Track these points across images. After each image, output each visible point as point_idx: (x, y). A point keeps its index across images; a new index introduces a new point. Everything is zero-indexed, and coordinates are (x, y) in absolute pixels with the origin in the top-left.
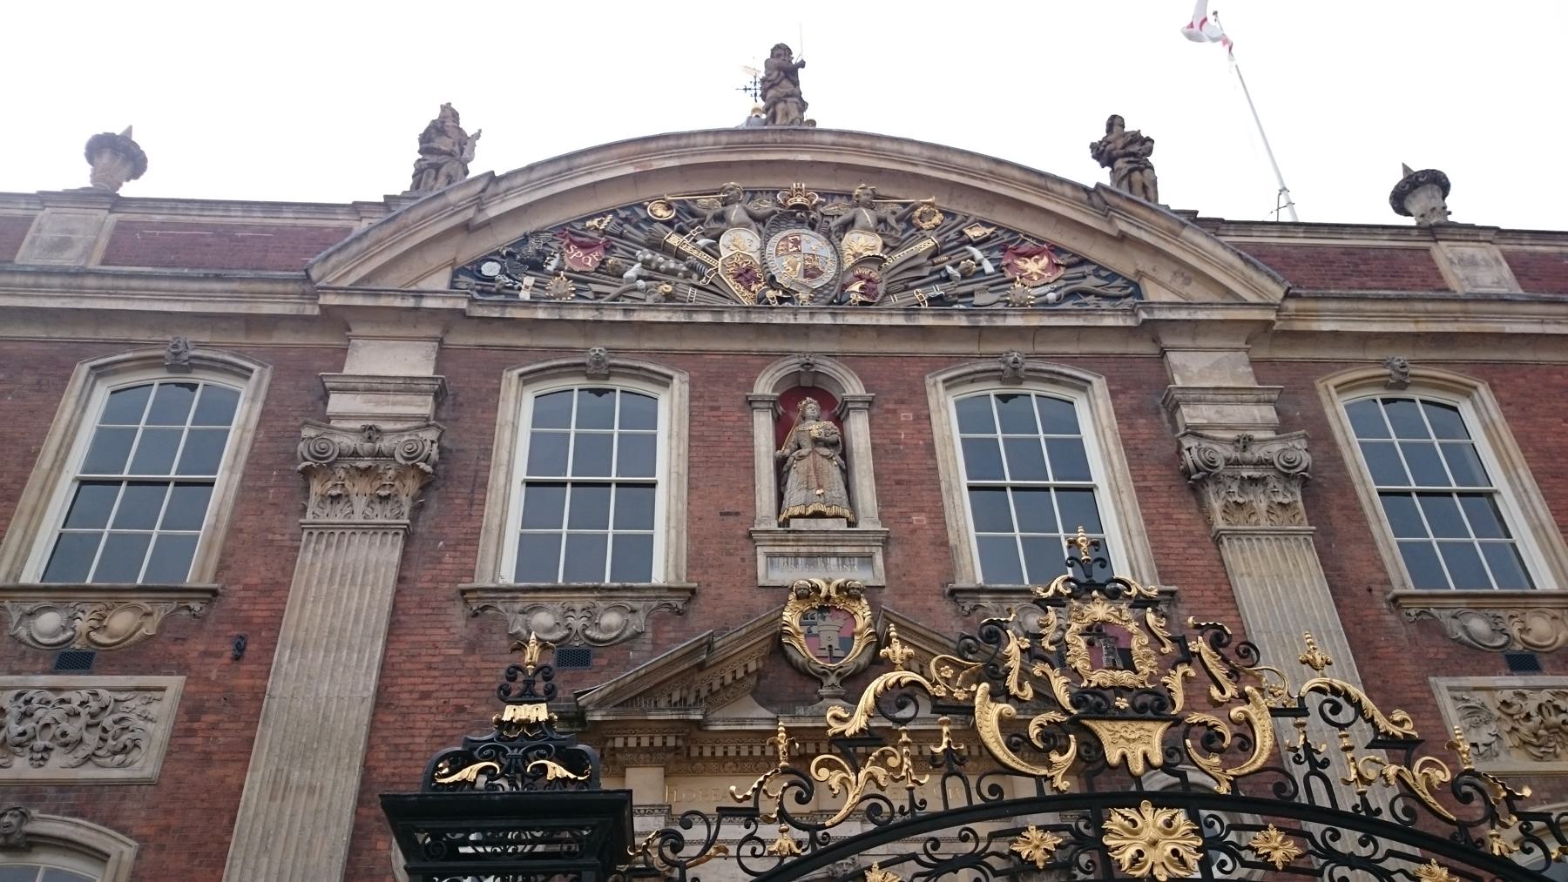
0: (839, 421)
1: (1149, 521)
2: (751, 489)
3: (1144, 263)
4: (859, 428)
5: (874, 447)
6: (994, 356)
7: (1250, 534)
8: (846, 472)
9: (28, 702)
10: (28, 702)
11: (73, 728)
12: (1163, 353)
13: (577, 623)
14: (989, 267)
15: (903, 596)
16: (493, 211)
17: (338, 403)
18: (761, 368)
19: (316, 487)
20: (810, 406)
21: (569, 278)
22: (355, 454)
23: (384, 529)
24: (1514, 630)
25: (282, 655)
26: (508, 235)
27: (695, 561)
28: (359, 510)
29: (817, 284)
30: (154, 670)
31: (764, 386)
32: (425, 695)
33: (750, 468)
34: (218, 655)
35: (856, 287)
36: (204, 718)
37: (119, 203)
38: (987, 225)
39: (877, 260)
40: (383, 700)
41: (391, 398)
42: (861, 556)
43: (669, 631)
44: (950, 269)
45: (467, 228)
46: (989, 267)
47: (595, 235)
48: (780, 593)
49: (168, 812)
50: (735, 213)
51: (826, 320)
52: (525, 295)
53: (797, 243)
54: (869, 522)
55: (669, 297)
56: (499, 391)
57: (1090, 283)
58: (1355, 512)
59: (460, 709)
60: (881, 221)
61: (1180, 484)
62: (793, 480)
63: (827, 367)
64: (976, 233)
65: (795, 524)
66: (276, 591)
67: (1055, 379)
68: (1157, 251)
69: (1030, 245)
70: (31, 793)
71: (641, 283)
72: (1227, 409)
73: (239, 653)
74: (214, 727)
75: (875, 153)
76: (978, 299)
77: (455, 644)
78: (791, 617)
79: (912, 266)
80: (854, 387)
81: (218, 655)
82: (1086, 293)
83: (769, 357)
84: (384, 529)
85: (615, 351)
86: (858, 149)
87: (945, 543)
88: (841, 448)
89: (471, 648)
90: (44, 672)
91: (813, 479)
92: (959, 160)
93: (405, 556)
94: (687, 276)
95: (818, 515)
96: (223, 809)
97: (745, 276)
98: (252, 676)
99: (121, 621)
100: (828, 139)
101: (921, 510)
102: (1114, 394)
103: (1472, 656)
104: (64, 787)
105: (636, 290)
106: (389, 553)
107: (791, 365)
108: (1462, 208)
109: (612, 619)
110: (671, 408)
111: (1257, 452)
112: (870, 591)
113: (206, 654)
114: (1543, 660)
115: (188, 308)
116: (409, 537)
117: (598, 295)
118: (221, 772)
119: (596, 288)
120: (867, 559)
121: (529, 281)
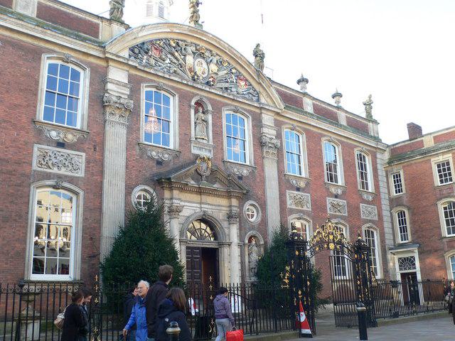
1: (254, 151)
3: (261, 90)
6: (234, 106)
9: (55, 154)
11: (67, 163)
12: (261, 113)
13: (161, 156)
17: (109, 86)
19: (108, 110)
23: (123, 124)
25: (107, 153)
26: (139, 41)
27: (180, 145)
28: (116, 118)
29: (204, 76)
30: (78, 150)
31: (193, 103)
33: (190, 124)
34: (91, 149)
35: (211, 79)
39: (217, 74)
40: (127, 167)
48: (197, 157)
50: (190, 49)
52: (144, 61)
55: (175, 72)
57: (251, 91)
62: (197, 128)
63: (204, 100)
64: (234, 71)
66: (102, 134)
67: (243, 114)
70: (59, 177)
71: (169, 65)
73: (95, 149)
75: (219, 43)
80: (210, 108)
81: (91, 149)
84: (123, 124)
86: (216, 41)
88: (205, 121)
97: (190, 70)
100: (211, 36)
104: (66, 176)
106: (123, 131)
108: (309, 89)
109: (166, 156)
110: (174, 103)
111: (273, 141)
115: (72, 46)
117: (160, 66)
120: (210, 151)
121: (145, 57)
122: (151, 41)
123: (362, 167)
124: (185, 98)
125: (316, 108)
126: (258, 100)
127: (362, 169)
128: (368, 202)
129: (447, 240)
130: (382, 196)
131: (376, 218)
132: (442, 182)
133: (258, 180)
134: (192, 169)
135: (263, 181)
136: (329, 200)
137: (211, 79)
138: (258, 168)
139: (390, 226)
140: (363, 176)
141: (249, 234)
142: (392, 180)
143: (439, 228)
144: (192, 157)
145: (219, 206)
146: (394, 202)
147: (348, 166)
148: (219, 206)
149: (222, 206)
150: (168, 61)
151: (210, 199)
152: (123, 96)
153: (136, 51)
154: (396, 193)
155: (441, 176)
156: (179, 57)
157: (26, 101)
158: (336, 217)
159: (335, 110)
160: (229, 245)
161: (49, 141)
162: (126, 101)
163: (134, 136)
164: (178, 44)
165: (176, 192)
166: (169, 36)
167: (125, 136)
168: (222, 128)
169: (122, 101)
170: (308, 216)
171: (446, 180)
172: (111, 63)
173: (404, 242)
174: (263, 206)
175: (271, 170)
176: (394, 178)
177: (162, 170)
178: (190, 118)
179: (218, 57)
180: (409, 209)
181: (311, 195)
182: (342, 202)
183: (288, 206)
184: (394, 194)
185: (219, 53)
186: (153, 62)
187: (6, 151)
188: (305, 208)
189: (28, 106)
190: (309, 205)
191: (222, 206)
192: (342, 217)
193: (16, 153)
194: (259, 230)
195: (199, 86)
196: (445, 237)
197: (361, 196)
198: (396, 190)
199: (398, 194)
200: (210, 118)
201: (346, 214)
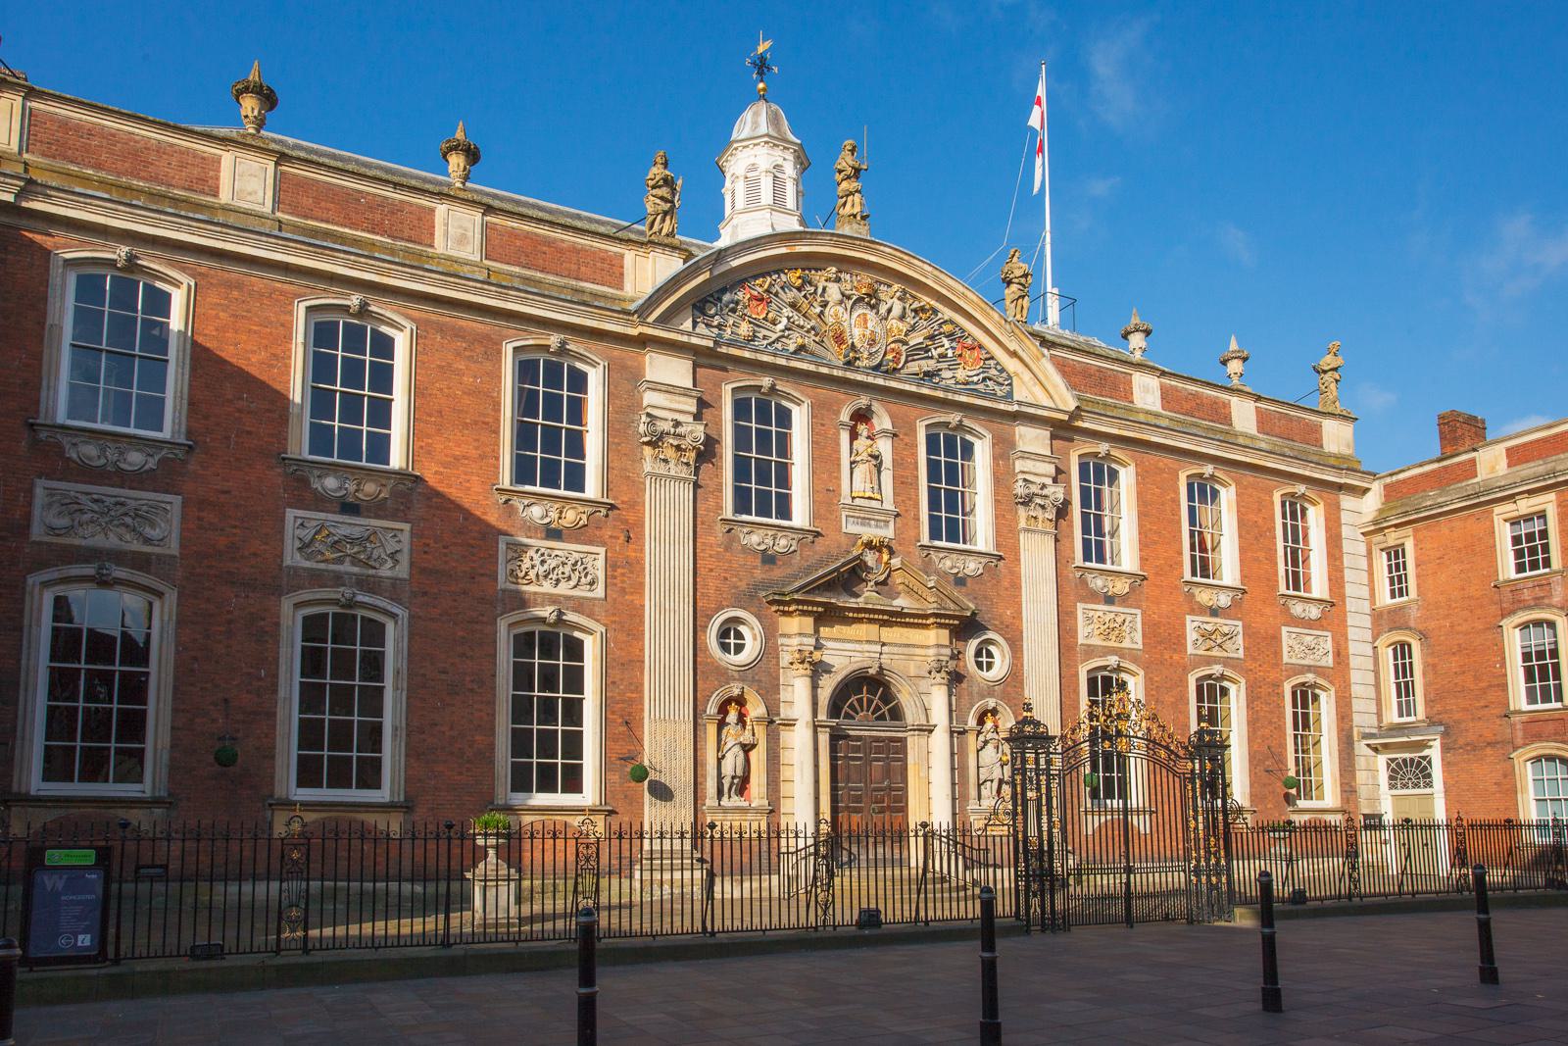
1: (996, 518)
2: (838, 478)
7: (1034, 531)
9: (543, 555)
10: (543, 555)
14: (950, 353)
15: (900, 545)
21: (750, 322)
23: (685, 480)
24: (1111, 585)
27: (815, 515)
30: (590, 543)
31: (845, 416)
32: (711, 570)
33: (839, 465)
35: (890, 357)
36: (619, 570)
41: (677, 398)
42: (884, 521)
43: (807, 553)
47: (760, 290)
48: (857, 536)
49: (614, 615)
52: (729, 331)
53: (866, 321)
54: (889, 505)
55: (802, 348)
56: (721, 397)
57: (993, 372)
59: (726, 579)
61: (1010, 501)
65: (858, 502)
66: (636, 505)
68: (1027, 366)
69: (969, 341)
71: (787, 333)
72: (1038, 464)
74: (623, 575)
77: (719, 546)
82: (990, 379)
87: (918, 519)
89: (727, 548)
90: (542, 539)
91: (868, 477)
94: (808, 332)
95: (870, 498)
96: (637, 613)
98: (635, 551)
101: (910, 499)
103: (1093, 596)
105: (783, 336)
106: (686, 493)
109: (783, 542)
113: (611, 537)
114: (1116, 600)
116: (696, 486)
117: (765, 337)
118: (631, 598)
119: (765, 332)
123: (1296, 536)
126: (1010, 394)
127: (1296, 540)
128: (1309, 624)
129: (1524, 718)
130: (1351, 605)
131: (1329, 661)
132: (1520, 568)
133: (1006, 584)
135: (1016, 586)
136: (1192, 625)
137: (890, 357)
138: (1003, 559)
139: (1370, 678)
140: (1295, 558)
142: (1382, 562)
143: (1504, 687)
144: (844, 540)
145: (908, 646)
146: (1383, 621)
147: (1253, 535)
148: (908, 646)
149: (914, 646)
152: (681, 418)
154: (1393, 596)
155: (1519, 554)
157: (477, 448)
158: (1209, 661)
160: (931, 731)
162: (689, 429)
163: (712, 503)
169: (680, 430)
170: (1135, 660)
171: (1534, 566)
173: (1405, 719)
175: (1036, 558)
176: (1389, 559)
177: (777, 573)
178: (838, 452)
180: (1423, 636)
181: (1143, 613)
182: (1225, 625)
183: (1081, 640)
184: (1385, 599)
187: (445, 555)
188: (1126, 644)
189: (482, 457)
190: (1138, 636)
191: (914, 646)
192: (1226, 662)
193: (464, 557)
194: (1006, 697)
195: (859, 377)
196: (1520, 712)
197: (1286, 609)
198: (1393, 592)
199: (1398, 600)
200: (884, 447)
201: (1241, 654)
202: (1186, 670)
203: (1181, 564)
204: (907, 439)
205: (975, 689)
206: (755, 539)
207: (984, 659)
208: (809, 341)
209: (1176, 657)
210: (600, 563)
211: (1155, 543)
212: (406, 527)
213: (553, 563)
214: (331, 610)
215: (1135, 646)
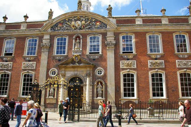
0: (80, 40)
4: (81, 40)
5: (82, 42)
8: (80, 45)
12: (107, 32)
14: (94, 24)
16: (53, 22)
17: (43, 41)
18: (74, 35)
20: (78, 39)
22: (45, 45)
31: (74, 37)
37: (27, 22)
38: (94, 19)
44: (91, 24)
45: (51, 24)
46: (94, 24)
50: (73, 20)
51: (79, 31)
52: (56, 29)
55: (67, 29)
58: (119, 47)
60: (86, 19)
63: (80, 35)
64: (93, 20)
65: (75, 50)
67: (98, 35)
76: (93, 27)
78: (74, 57)
79: (87, 24)
80: (81, 37)
83: (75, 34)
85: (63, 34)
92: (92, 13)
93: (48, 53)
97: (73, 26)
99: (32, 58)
102: (102, 36)
103: (124, 59)
104: (30, 69)
107: (76, 35)
112: (80, 55)
116: (49, 51)
120: (80, 52)
122: (59, 23)
124: (71, 36)
125: (144, 21)
134: (70, 60)
141: (97, 80)
148: (82, 71)
150: (65, 26)
151: (79, 69)
153: (53, 27)
156: (69, 24)
159: (160, 18)
161: (26, 61)
164: (69, 20)
165: (63, 69)
166: (66, 18)
167: (47, 54)
168: (87, 43)
172: (44, 34)
174: (106, 69)
179: (87, 17)
185: (86, 16)
186: (59, 28)
202: (148, 71)
203: (147, 51)
204: (85, 39)
205: (97, 77)
206: (57, 58)
207: (100, 72)
208: (69, 28)
209: (145, 69)
210: (35, 64)
211: (140, 48)
212: (12, 62)
213: (29, 65)
214: (4, 73)
215: (134, 67)
